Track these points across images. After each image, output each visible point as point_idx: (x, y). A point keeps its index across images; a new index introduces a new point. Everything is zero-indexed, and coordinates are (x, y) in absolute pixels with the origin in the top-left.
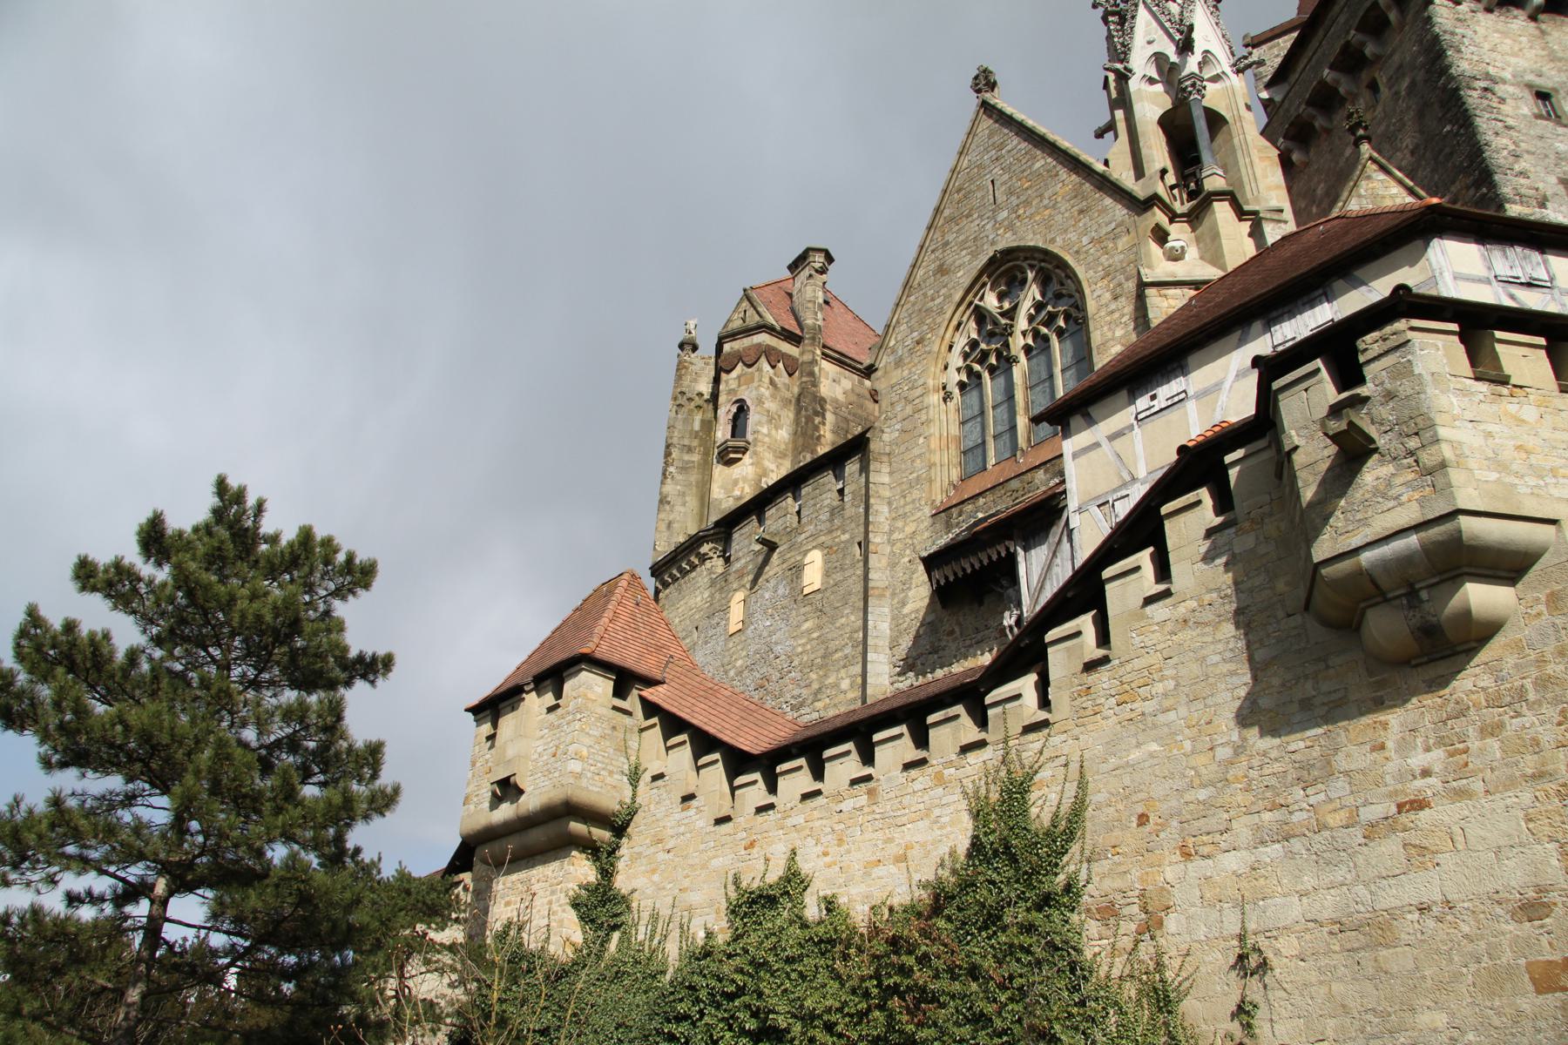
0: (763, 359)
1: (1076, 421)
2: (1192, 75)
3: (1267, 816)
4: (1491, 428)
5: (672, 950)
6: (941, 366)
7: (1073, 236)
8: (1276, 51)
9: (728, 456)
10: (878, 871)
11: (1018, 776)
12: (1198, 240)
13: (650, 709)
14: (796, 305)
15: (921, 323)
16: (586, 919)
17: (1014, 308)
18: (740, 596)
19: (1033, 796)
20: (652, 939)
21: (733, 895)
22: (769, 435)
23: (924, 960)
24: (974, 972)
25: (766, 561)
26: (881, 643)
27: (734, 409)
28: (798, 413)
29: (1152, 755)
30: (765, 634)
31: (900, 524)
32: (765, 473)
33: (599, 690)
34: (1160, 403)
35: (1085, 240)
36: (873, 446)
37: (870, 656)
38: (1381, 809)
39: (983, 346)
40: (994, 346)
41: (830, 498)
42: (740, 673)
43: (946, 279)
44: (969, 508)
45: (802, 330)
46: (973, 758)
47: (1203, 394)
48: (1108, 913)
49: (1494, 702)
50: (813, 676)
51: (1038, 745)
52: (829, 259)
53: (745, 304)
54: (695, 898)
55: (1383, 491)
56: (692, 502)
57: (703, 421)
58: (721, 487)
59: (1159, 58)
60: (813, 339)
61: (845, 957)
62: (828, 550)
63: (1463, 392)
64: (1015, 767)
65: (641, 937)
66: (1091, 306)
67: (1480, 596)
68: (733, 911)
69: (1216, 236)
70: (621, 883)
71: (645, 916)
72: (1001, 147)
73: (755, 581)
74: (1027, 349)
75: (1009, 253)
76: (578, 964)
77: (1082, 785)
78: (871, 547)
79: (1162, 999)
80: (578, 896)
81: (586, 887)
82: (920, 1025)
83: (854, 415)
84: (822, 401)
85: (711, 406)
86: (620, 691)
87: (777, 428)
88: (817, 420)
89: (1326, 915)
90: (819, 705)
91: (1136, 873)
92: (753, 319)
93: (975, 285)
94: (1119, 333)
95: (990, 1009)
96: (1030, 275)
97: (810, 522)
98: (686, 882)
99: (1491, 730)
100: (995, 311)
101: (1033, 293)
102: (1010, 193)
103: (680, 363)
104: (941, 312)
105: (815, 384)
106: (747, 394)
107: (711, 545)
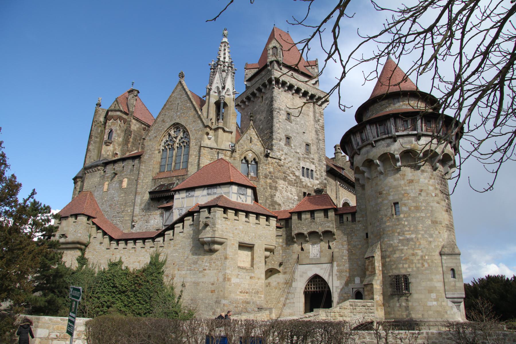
0: (118, 119)
1: (177, 193)
2: (223, 96)
3: (189, 267)
4: (223, 225)
5: (97, 270)
6: (159, 145)
7: (191, 126)
8: (250, 72)
9: (107, 144)
10: (135, 263)
11: (158, 253)
12: (215, 135)
13: (94, 224)
14: (128, 103)
15: (157, 132)
16: (79, 262)
17: (177, 137)
18: (107, 183)
19: (160, 257)
20: (92, 267)
21: (109, 262)
22: (117, 140)
23: (141, 279)
24: (148, 282)
25: (114, 177)
26: (138, 204)
27: (109, 131)
28: (125, 134)
29: (176, 255)
30: (112, 194)
31: (145, 179)
32: (115, 149)
33: (85, 220)
34: (190, 195)
35: (193, 129)
36: (142, 159)
37: (135, 207)
38: (201, 269)
39: (169, 143)
40: (171, 144)
41: (130, 167)
42: (105, 201)
43: (164, 124)
44: (160, 180)
45: (129, 112)
46: (152, 249)
47: (197, 197)
48: (167, 276)
49: (216, 259)
50: (122, 207)
51: (161, 250)
52: (138, 92)
53: (116, 102)
54: (102, 262)
55: (208, 231)
56: (96, 151)
57: (101, 130)
58: (104, 151)
59: (218, 88)
60: (131, 115)
61: (129, 276)
62: (129, 180)
63: (221, 220)
64: (158, 252)
65: (90, 267)
66: (191, 145)
67: (216, 247)
68: (109, 265)
69: (218, 137)
70: (86, 256)
71: (91, 263)
72: (182, 95)
73: (111, 180)
74: (178, 147)
75: (178, 124)
76: (78, 271)
77: (167, 257)
78: (138, 183)
79: (172, 288)
80: (78, 258)
81: (79, 256)
82: (140, 288)
83: (138, 134)
84: (131, 132)
85: (104, 126)
86: (88, 220)
87: (120, 137)
88: (129, 137)
89: (193, 281)
90: (123, 214)
91: (172, 271)
92: (117, 108)
93: (170, 128)
94: (195, 153)
95: (150, 288)
96: (181, 130)
97: (125, 171)
98: (100, 259)
99: (214, 263)
100: (173, 136)
101: (181, 135)
102: (181, 109)
103: (96, 110)
104: (161, 132)
105: (130, 127)
106: (114, 128)
107: (101, 167)
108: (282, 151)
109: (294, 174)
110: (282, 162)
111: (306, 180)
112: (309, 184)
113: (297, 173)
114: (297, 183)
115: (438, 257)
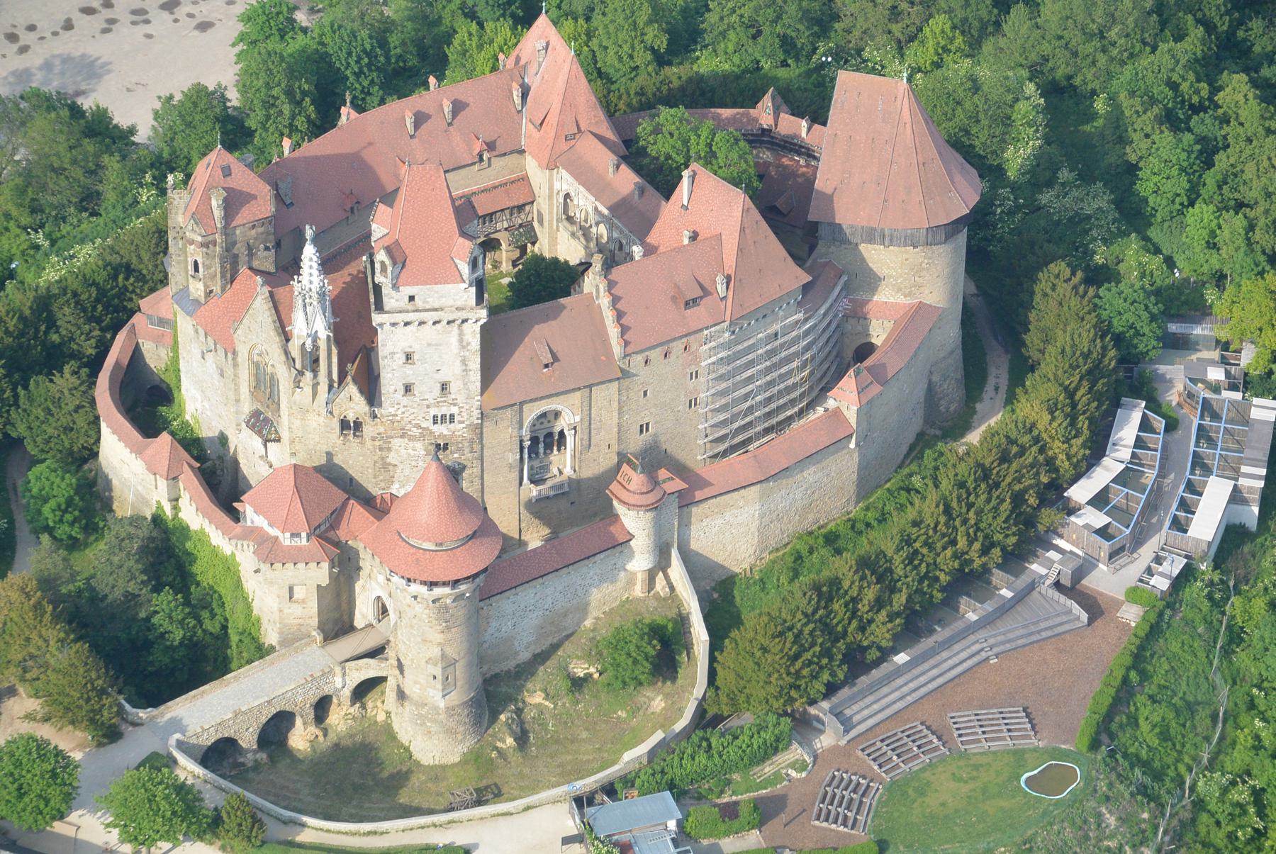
108: (399, 404)
109: (418, 427)
110: (398, 418)
111: (442, 430)
112: (446, 432)
113: (424, 425)
114: (424, 436)
115: (423, 663)
